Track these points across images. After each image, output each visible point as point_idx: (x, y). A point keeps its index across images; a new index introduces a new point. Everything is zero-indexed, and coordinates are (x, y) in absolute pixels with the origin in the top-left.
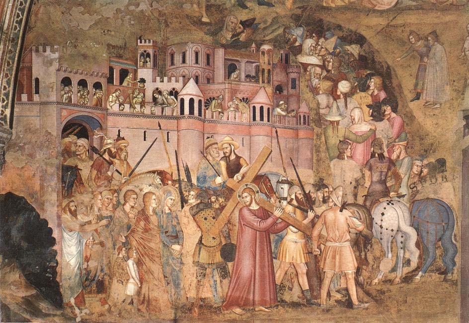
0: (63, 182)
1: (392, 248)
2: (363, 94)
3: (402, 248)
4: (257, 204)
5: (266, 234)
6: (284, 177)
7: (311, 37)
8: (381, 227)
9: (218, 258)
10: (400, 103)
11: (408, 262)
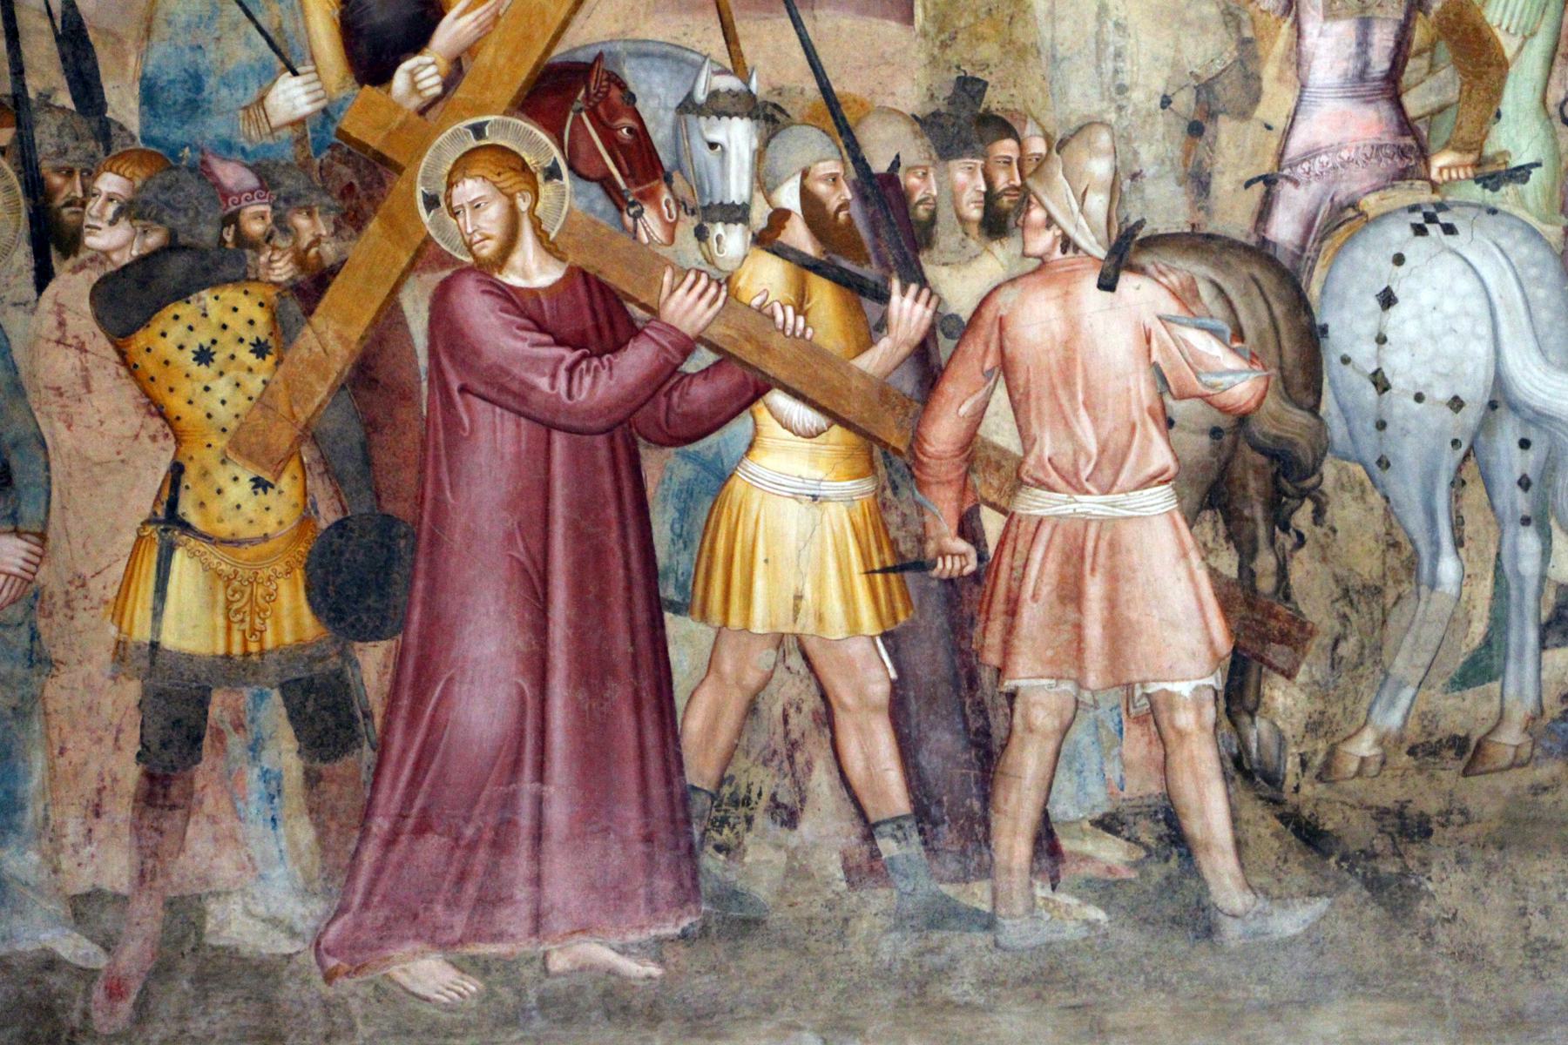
1: (1457, 524)
3: (1526, 521)
4: (549, 247)
5: (613, 450)
6: (724, 72)
8: (1380, 383)
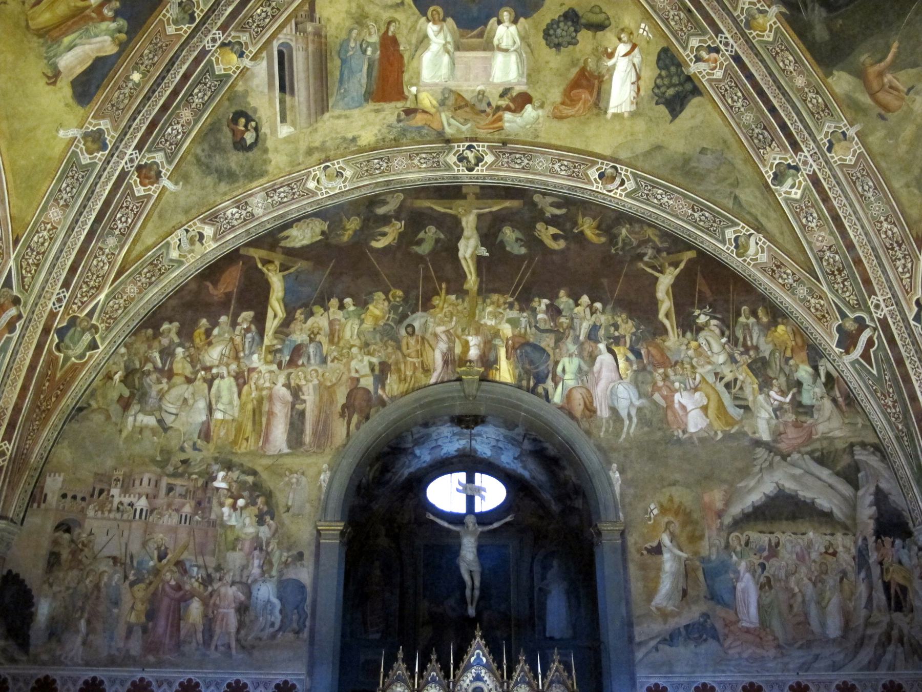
0: (49, 562)
2: (253, 508)
7: (223, 470)
9: (143, 619)
10: (276, 514)
11: (273, 625)
